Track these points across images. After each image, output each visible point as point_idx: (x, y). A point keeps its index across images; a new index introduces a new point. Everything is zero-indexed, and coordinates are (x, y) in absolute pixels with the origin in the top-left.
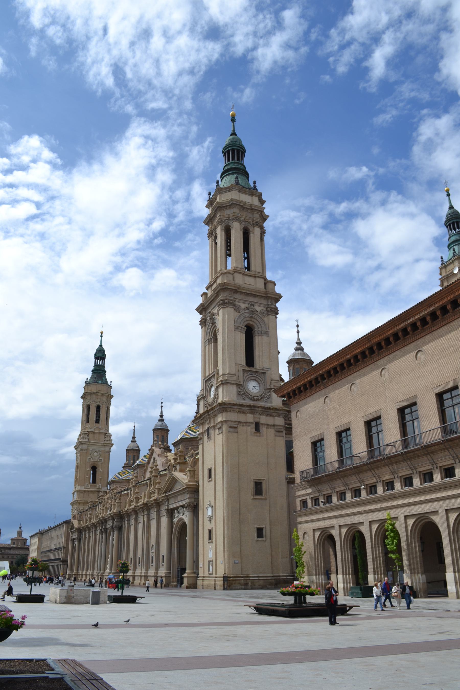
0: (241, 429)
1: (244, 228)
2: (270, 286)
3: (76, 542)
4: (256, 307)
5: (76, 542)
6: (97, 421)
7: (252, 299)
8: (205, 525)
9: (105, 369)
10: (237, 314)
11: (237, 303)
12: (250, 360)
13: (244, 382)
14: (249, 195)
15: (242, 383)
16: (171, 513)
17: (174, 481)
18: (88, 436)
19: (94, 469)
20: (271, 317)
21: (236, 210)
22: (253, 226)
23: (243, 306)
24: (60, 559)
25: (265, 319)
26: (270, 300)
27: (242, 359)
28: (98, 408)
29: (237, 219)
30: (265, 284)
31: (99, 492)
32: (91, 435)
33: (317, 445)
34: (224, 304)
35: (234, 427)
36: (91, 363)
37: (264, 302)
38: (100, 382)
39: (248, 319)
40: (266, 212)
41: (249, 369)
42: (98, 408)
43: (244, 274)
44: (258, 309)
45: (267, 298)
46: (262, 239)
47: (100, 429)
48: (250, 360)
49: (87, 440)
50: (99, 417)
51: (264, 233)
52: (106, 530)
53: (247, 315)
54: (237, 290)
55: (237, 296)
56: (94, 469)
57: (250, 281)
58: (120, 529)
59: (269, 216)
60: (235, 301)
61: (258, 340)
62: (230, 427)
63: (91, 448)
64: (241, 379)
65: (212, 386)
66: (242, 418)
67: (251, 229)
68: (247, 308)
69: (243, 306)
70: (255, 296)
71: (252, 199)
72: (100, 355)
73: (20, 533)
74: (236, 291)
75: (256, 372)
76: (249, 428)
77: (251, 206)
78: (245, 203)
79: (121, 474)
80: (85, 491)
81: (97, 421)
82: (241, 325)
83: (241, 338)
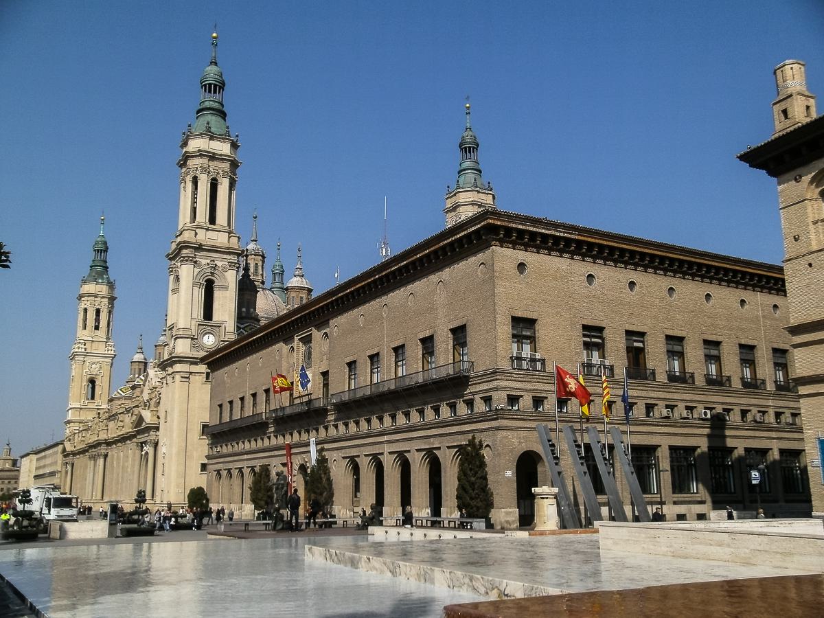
1: (212, 179)
4: (216, 262)
6: (97, 328)
10: (197, 270)
12: (208, 314)
17: (141, 419)
18: (85, 345)
19: (92, 382)
21: (205, 161)
23: (204, 262)
27: (199, 312)
28: (98, 312)
29: (205, 170)
31: (98, 409)
32: (88, 344)
34: (186, 260)
35: (187, 377)
38: (100, 281)
39: (209, 274)
41: (207, 322)
42: (98, 312)
44: (219, 264)
45: (230, 253)
48: (208, 314)
49: (83, 350)
50: (99, 323)
53: (209, 270)
54: (199, 248)
56: (92, 382)
60: (195, 258)
62: (182, 377)
63: (89, 359)
66: (194, 369)
69: (204, 262)
77: (221, 155)
78: (214, 154)
80: (81, 409)
81: (97, 328)
82: (201, 281)
83: (200, 294)
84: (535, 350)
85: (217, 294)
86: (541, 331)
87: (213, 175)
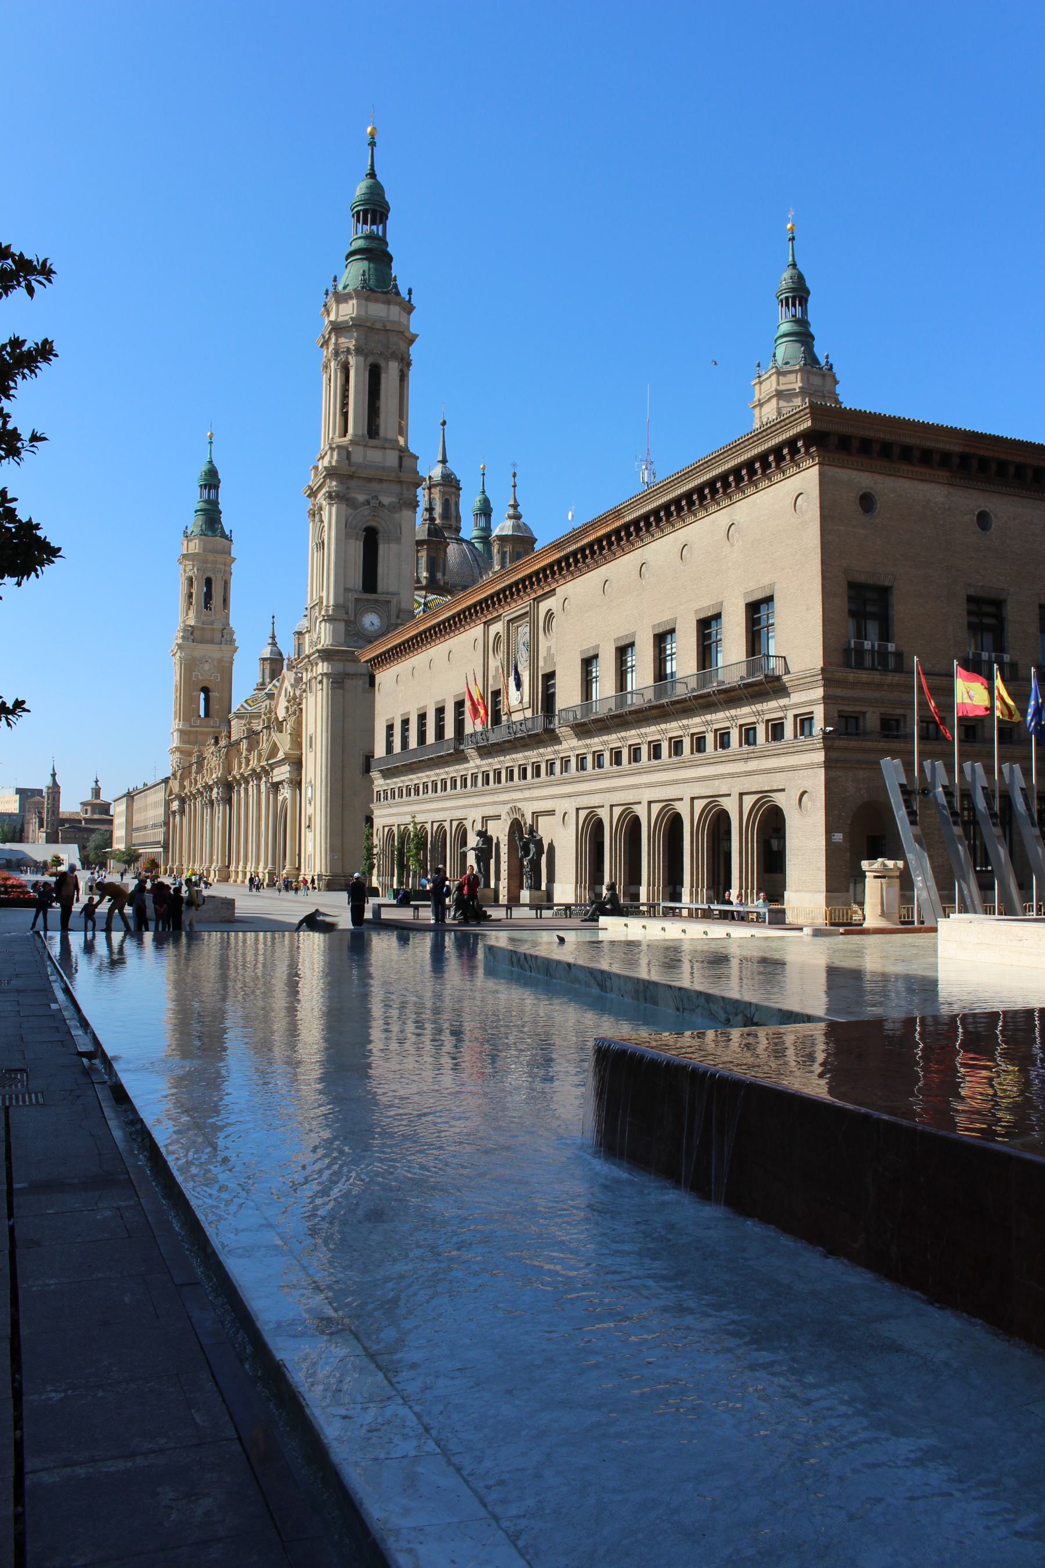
0: (349, 683)
2: (406, 462)
3: (178, 817)
5: (178, 817)
7: (375, 486)
8: (308, 810)
9: (220, 507)
10: (350, 511)
11: (353, 495)
13: (356, 616)
14: (383, 302)
15: (352, 619)
16: (276, 787)
20: (406, 513)
22: (387, 359)
23: (361, 498)
24: (158, 843)
25: (397, 516)
26: (405, 486)
27: (356, 579)
30: (401, 458)
33: (390, 728)
36: (194, 499)
37: (395, 488)
40: (413, 330)
43: (365, 446)
44: (386, 500)
46: (403, 377)
47: (212, 623)
51: (409, 364)
52: (211, 802)
53: (366, 512)
55: (353, 483)
57: (375, 456)
58: (229, 801)
59: (417, 336)
61: (383, 549)
64: (351, 611)
65: (316, 618)
67: (382, 364)
68: (368, 503)
70: (381, 481)
71: (388, 309)
72: (211, 481)
73: (97, 792)
74: (351, 477)
75: (376, 601)
76: (360, 683)
79: (250, 702)
83: (357, 549)
84: (885, 635)
85: (382, 549)
86: (901, 610)
87: (370, 360)
